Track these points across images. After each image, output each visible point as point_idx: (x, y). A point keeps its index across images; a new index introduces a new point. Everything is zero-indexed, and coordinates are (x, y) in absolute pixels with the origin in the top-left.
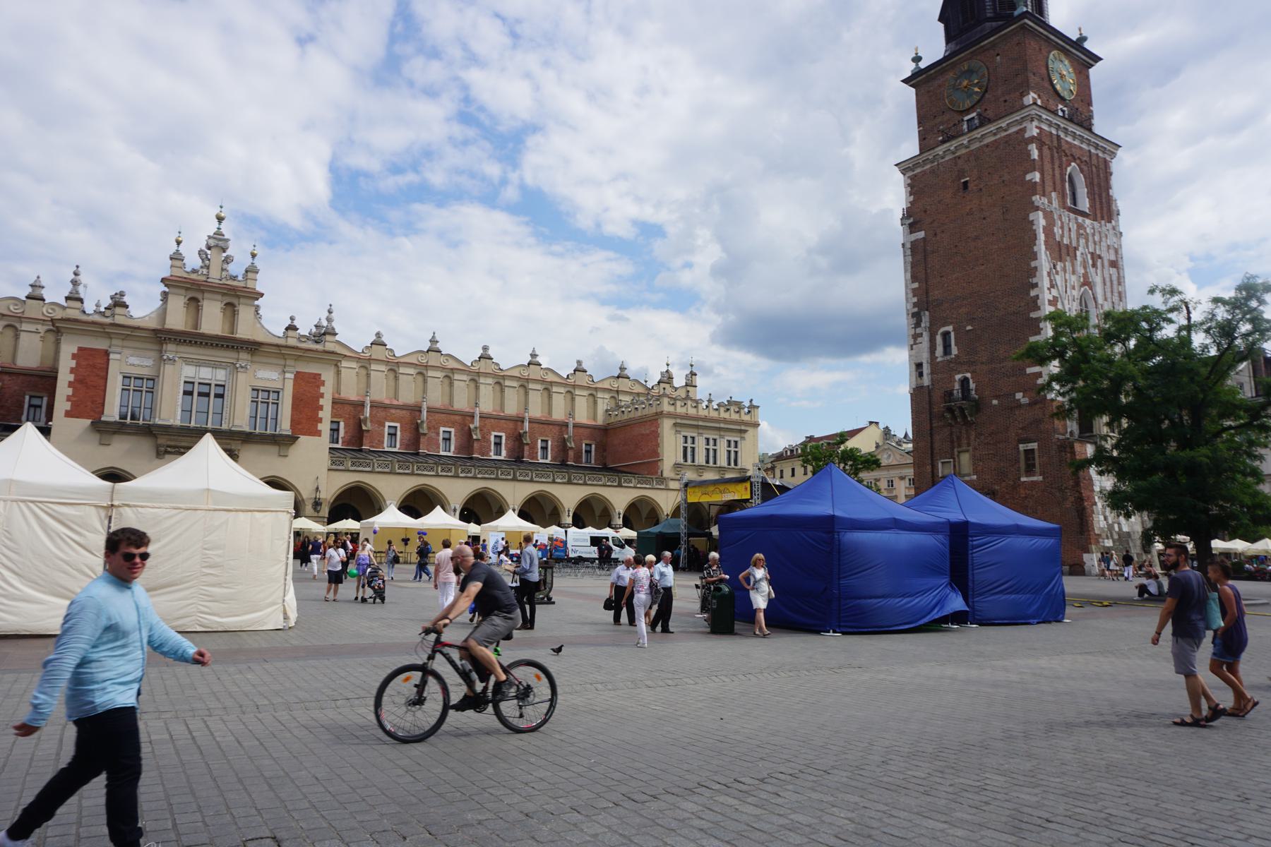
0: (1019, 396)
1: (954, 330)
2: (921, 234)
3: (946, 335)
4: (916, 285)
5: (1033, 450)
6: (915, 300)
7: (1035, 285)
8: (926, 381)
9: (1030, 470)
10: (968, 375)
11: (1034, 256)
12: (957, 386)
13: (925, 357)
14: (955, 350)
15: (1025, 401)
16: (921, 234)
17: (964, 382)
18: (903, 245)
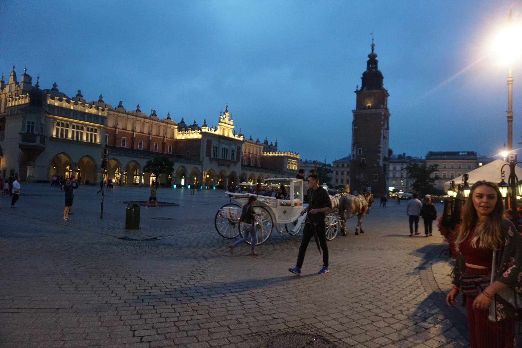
0: (375, 165)
1: (362, 149)
2: (356, 127)
3: (360, 150)
4: (354, 138)
5: (377, 175)
6: (354, 141)
7: (380, 144)
8: (355, 158)
9: (376, 179)
10: (364, 159)
11: (381, 138)
12: (361, 161)
13: (355, 153)
14: (362, 153)
15: (376, 166)
16: (356, 127)
17: (363, 160)
18: (352, 129)
